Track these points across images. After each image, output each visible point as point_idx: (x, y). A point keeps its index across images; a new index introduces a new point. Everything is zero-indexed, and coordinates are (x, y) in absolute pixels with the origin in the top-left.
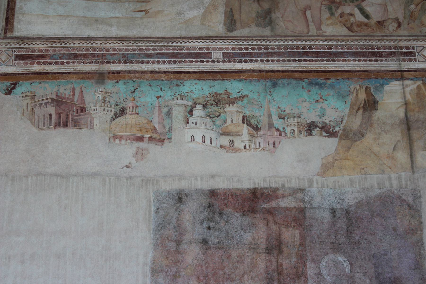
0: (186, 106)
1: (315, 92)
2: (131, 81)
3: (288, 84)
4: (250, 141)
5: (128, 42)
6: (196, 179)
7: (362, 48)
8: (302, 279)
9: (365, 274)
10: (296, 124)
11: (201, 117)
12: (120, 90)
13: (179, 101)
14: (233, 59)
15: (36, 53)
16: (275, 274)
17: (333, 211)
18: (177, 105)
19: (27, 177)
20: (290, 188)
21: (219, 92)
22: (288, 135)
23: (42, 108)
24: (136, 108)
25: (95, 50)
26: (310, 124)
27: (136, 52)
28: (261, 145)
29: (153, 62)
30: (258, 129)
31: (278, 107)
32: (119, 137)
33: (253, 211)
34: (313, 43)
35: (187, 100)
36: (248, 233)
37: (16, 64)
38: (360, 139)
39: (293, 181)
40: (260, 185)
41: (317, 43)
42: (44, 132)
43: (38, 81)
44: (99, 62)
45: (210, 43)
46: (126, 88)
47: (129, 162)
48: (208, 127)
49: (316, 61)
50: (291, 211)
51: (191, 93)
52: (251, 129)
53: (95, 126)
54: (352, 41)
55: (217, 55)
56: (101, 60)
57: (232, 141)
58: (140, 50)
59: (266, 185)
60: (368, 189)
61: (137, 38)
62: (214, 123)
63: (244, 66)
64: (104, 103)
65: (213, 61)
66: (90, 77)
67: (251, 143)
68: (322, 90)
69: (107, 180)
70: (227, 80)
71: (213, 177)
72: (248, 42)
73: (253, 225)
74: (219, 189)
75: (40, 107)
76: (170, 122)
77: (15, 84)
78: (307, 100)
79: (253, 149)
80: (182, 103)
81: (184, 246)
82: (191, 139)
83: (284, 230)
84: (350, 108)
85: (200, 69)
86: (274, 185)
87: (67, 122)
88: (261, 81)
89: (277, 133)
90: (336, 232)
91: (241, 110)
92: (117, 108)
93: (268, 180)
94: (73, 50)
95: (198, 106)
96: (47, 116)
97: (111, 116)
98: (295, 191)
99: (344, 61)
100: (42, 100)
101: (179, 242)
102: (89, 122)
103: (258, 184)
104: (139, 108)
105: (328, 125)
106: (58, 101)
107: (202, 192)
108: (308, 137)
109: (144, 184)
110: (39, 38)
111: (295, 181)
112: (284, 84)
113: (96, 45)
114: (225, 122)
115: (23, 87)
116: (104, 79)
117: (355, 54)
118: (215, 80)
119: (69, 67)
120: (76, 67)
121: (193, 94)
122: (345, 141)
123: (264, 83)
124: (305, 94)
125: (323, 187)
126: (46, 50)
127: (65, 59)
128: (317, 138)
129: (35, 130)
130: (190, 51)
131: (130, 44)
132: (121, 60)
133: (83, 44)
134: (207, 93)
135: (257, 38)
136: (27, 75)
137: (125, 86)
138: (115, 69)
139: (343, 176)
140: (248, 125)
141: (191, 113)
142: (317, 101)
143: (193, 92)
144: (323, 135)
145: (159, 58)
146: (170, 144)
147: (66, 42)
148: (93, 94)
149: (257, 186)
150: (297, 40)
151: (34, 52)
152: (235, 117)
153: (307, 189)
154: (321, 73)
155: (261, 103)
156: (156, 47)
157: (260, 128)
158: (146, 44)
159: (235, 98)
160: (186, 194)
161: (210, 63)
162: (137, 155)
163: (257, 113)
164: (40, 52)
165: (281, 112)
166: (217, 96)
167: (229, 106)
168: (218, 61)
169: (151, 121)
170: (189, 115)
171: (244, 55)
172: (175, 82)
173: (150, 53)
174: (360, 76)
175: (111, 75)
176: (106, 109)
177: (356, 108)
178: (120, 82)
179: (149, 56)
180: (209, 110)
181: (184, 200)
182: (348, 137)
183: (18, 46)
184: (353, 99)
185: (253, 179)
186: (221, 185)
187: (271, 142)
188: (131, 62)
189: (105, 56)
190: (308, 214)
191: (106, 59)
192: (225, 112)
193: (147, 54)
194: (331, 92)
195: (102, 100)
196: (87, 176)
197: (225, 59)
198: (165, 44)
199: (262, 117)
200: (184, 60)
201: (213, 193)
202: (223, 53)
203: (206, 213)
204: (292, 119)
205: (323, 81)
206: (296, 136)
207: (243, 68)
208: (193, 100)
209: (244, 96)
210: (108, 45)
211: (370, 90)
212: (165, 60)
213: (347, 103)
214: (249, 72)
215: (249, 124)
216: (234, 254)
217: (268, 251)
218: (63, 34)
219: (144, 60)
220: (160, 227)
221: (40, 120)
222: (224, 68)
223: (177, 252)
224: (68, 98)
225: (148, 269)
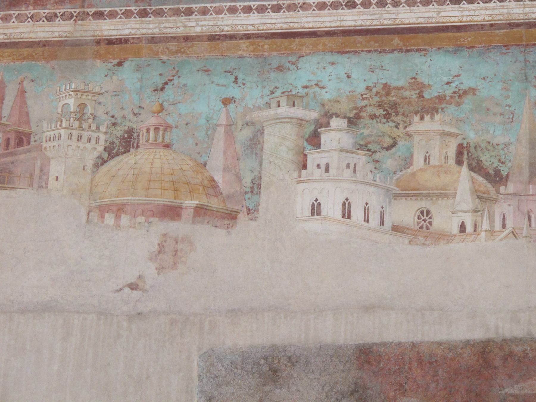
0: (301, 122)
4: (476, 211)
11: (342, 150)
13: (285, 110)
18: (278, 120)
21: (394, 84)
24: (165, 130)
28: (507, 222)
29: (219, 11)
30: (501, 179)
32: (115, 208)
35: (307, 107)
40: (500, 331)
44: (72, 16)
46: (141, 80)
47: (137, 274)
48: (359, 176)
51: (317, 89)
52: (480, 179)
53: (52, 182)
56: (78, 10)
57: (425, 213)
59: (519, 332)
62: (378, 165)
63: (466, 13)
66: (46, 54)
67: (479, 219)
70: (419, 50)
71: (368, 309)
74: (384, 344)
80: (292, 115)
82: (313, 209)
85: (344, 24)
91: (454, 130)
92: (115, 132)
95: (335, 122)
97: (96, 154)
102: (37, 172)
103: (497, 328)
104: (174, 130)
107: (336, 352)
114: (408, 161)
118: (384, 51)
120: (11, 31)
121: (324, 91)
123: (521, 58)
132: (133, 8)
134: (361, 88)
137: (138, 75)
138: (114, 33)
140: (471, 168)
141: (314, 140)
143: (321, 84)
146: (253, 224)
149: (491, 335)
152: (437, 150)
155: (512, 109)
157: (507, 176)
159: (438, 97)
160: (290, 358)
162: (160, 256)
163: (498, 135)
166: (388, 94)
167: (422, 118)
169: (205, 165)
170: (309, 147)
175: (103, 46)
176: (86, 135)
178: (126, 64)
180: (366, 132)
181: (285, 374)
186: (392, 330)
188: (159, 13)
191: (91, 6)
192: (410, 136)
195: (75, 113)
196: (23, 312)
199: (512, 148)
201: (366, 355)
207: (465, 19)
208: (323, 105)
209: (465, 92)
212: (251, 4)
215: (477, 167)
219: (194, 6)
222: (412, 21)
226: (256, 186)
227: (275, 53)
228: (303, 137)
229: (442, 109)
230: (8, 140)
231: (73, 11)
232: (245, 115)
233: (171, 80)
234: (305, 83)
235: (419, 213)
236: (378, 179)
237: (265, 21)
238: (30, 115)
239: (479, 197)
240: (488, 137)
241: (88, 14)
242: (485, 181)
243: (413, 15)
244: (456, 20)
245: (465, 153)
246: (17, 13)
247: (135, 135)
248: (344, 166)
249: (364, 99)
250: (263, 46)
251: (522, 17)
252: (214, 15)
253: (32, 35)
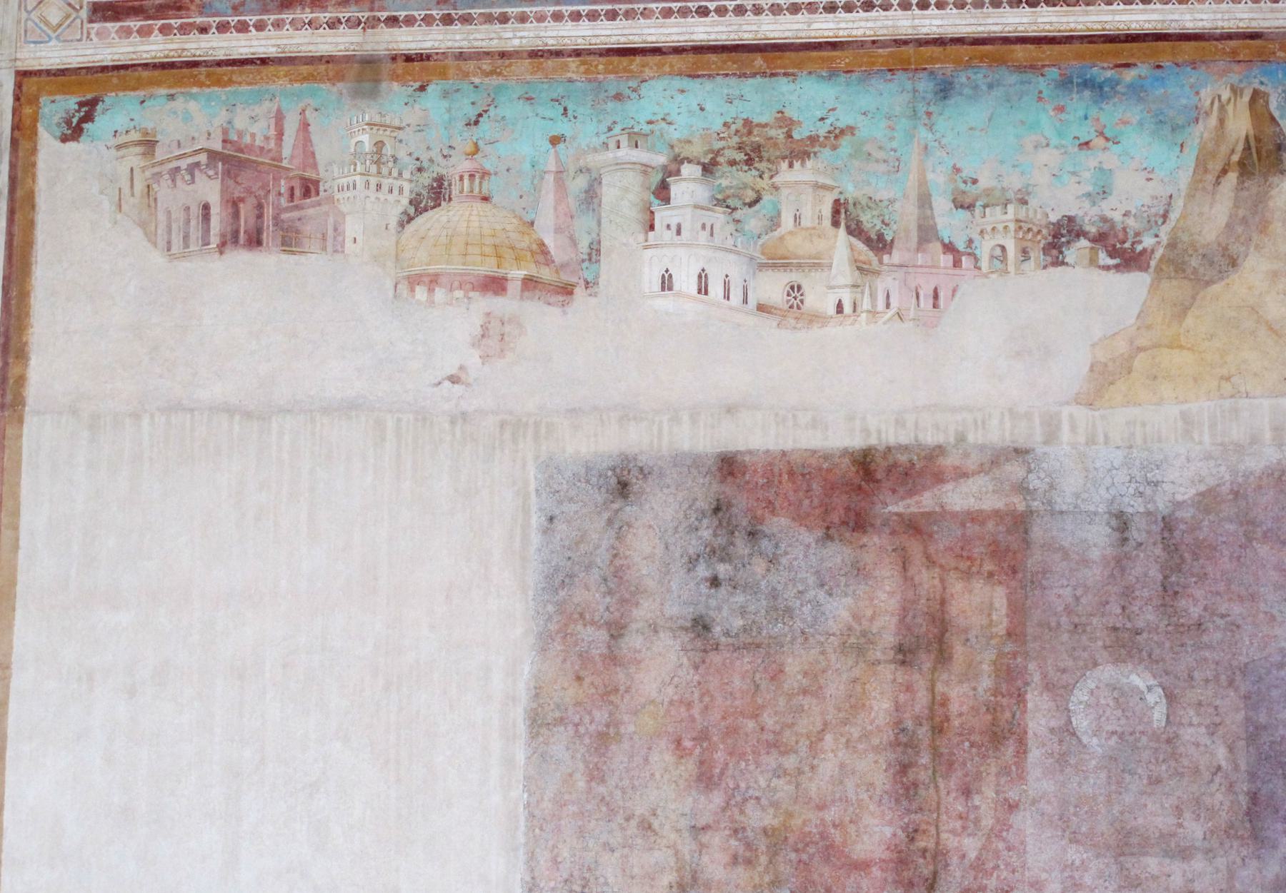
0: (646, 169)
1: (1081, 113)
2: (465, 86)
3: (990, 86)
6: (675, 419)
8: (1009, 750)
9: (1213, 729)
10: (1012, 226)
11: (696, 207)
13: (626, 153)
16: (923, 732)
17: (1122, 523)
18: (619, 165)
19: (136, 416)
20: (982, 448)
21: (756, 121)
22: (984, 264)
23: (179, 182)
24: (482, 178)
26: (1058, 225)
28: (892, 300)
29: (541, 18)
30: (885, 246)
31: (954, 167)
32: (426, 280)
33: (859, 523)
35: (652, 149)
36: (841, 596)
37: (93, 36)
38: (1222, 275)
39: (995, 422)
40: (883, 436)
42: (185, 265)
43: (163, 91)
46: (449, 110)
47: (457, 366)
48: (717, 240)
50: (983, 523)
51: (663, 124)
52: (860, 246)
53: (349, 244)
56: (367, 14)
57: (795, 289)
59: (904, 438)
60: (1239, 448)
62: (739, 226)
63: (843, 25)
64: (378, 162)
67: (859, 296)
68: (1103, 106)
69: (390, 424)
70: (785, 74)
71: (730, 410)
73: (859, 571)
74: (750, 452)
75: (173, 180)
76: (594, 224)
77: (93, 103)
78: (1054, 141)
79: (864, 315)
80: (634, 160)
81: (633, 641)
82: (663, 282)
83: (957, 587)
84: (1197, 166)
85: (694, 37)
86: (930, 438)
87: (259, 231)
88: (900, 75)
89: (946, 260)
90: (1128, 593)
91: (829, 182)
92: (421, 180)
93: (910, 419)
95: (687, 169)
96: (196, 211)
97: (401, 209)
98: (998, 457)
100: (179, 157)
101: (616, 630)
102: (330, 232)
103: (879, 432)
104: (493, 177)
105: (1119, 227)
106: (231, 160)
107: (694, 462)
108: (1051, 269)
109: (507, 435)
111: (1002, 422)
112: (976, 87)
114: (774, 222)
115: (119, 114)
116: (377, 81)
118: (744, 75)
119: (263, 42)
120: (285, 41)
122: (1174, 283)
124: (1046, 119)
125: (1091, 441)
127: (252, 12)
128: (1079, 272)
129: (157, 258)
132: (434, 13)
134: (717, 125)
136: (129, 72)
137: (445, 104)
138: (413, 46)
139: (1160, 402)
140: (850, 232)
141: (663, 192)
142: (1087, 143)
143: (669, 119)
144: (1101, 263)
146: (593, 300)
148: (341, 134)
149: (873, 441)
152: (809, 207)
153: (1040, 450)
154: (1102, 46)
155: (898, 154)
157: (892, 241)
159: (810, 138)
160: (641, 469)
162: (484, 341)
163: (883, 191)
165: (962, 186)
166: (750, 133)
167: (791, 166)
169: (532, 223)
170: (657, 202)
172: (613, 84)
174: (1234, 52)
175: (401, 64)
176: (386, 182)
177: (1216, 166)
178: (430, 89)
181: (636, 488)
182: (1184, 271)
184: (1206, 135)
185: (864, 419)
186: (756, 436)
187: (926, 291)
188: (466, 20)
190: (1037, 533)
191: (382, 9)
192: (776, 188)
194: (1135, 113)
195: (373, 153)
196: (326, 411)
199: (897, 205)
200: (642, 6)
201: (729, 466)
203: (706, 534)
204: (998, 208)
205: (1109, 74)
206: (1011, 268)
207: (841, 33)
208: (672, 147)
209: (842, 132)
211: (1267, 103)
212: (580, 8)
213: (1186, 150)
214: (862, 44)
215: (856, 230)
216: (793, 667)
217: (904, 655)
219: (509, 10)
220: (559, 580)
221: (174, 226)
223: (613, 659)
224: (262, 148)
225: (519, 715)
226: (594, 253)
227: (612, 76)
228: (649, 189)
229: (815, 153)
230: (292, 189)
231: (360, 15)
232: (578, 159)
233: (486, 111)
234: (650, 118)
235: (788, 288)
236: (739, 245)
237: (598, 32)
238: (318, 156)
239: (858, 268)
240: (868, 191)
242: (866, 248)
243: (778, 27)
244: (831, 34)
245: (843, 211)
246: (291, 17)
247: (446, 183)
248: (699, 226)
249: (722, 139)
250: (596, 66)
251: (910, 31)
252: (535, 24)
253: (311, 48)
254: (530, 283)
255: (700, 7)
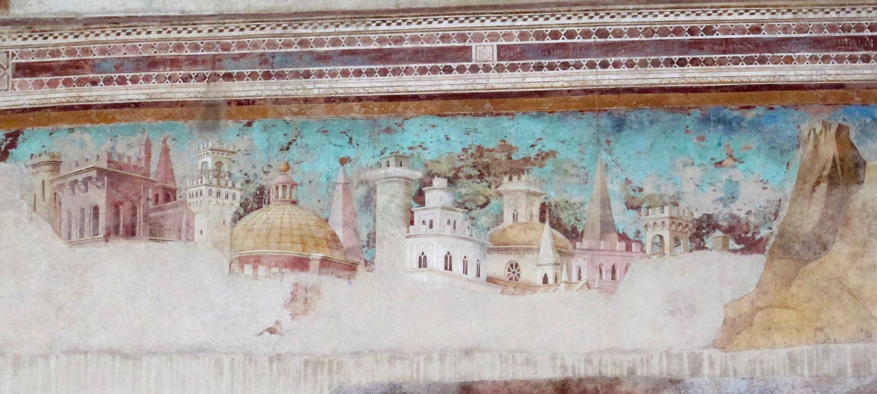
0: (407, 181)
1: (716, 142)
2: (280, 123)
3: (652, 122)
4: (556, 264)
5: (274, 25)
6: (429, 359)
7: (832, 28)
10: (667, 222)
11: (443, 208)
12: (251, 147)
13: (394, 170)
14: (521, 62)
15: (61, 59)
18: (388, 179)
19: (46, 357)
20: (647, 379)
21: (487, 146)
22: (648, 248)
23: (77, 191)
25: (196, 47)
26: (700, 221)
27: (293, 50)
29: (333, 75)
31: (626, 179)
32: (252, 260)
34: (714, 17)
35: (412, 167)
37: (16, 87)
38: (817, 256)
39: (655, 361)
40: (577, 371)
41: (725, 17)
42: (81, 250)
43: (66, 126)
44: (205, 78)
45: (467, 24)
46: (268, 140)
47: (274, 321)
48: (459, 232)
49: (722, 62)
51: (420, 150)
52: (559, 235)
53: (197, 234)
54: (810, 10)
55: (484, 52)
56: (210, 72)
57: (514, 266)
58: (302, 43)
59: (591, 372)
60: (829, 379)
61: (296, 14)
62: (474, 222)
63: (547, 79)
64: (217, 177)
65: (474, 69)
66: (184, 114)
67: (559, 271)
68: (732, 136)
69: (226, 362)
70: (507, 114)
71: (468, 352)
72: (558, 19)
74: (482, 382)
75: (73, 190)
76: (371, 221)
78: (697, 162)
79: (562, 285)
80: (400, 175)
82: (420, 262)
84: (799, 178)
85: (442, 88)
87: (133, 226)
88: (588, 114)
89: (620, 246)
91: (538, 190)
92: (249, 189)
93: (596, 359)
94: (146, 48)
95: (437, 182)
96: (89, 211)
97: (234, 210)
98: (658, 385)
99: (789, 60)
100: (77, 173)
102: (184, 226)
103: (574, 368)
104: (299, 187)
105: (743, 222)
106: (113, 175)
108: (695, 252)
109: (310, 371)
110: (68, 21)
111: (661, 361)
112: (641, 123)
113: (198, 35)
114: (499, 218)
115: (34, 143)
116: (218, 119)
117: (817, 43)
118: (476, 115)
119: (137, 92)
120: (152, 91)
121: (427, 152)
122: (783, 261)
123: (594, 122)
124: (691, 146)
125: (724, 374)
126: (83, 49)
128: (715, 254)
129: (60, 245)
130: (420, 45)
131: (279, 30)
132: (257, 70)
133: (169, 32)
134: (458, 150)
135: (579, 8)
136: (42, 112)
137: (265, 135)
138: (243, 94)
139: (773, 346)
140: (553, 226)
141: (420, 198)
142: (720, 163)
143: (424, 146)
144: (731, 247)
145: (346, 64)
146: (370, 275)
147: (129, 30)
148: (192, 157)
149: (569, 374)
150: (677, 11)
151: (58, 56)
152: (524, 207)
153: (688, 380)
154: (731, 94)
155: (587, 170)
156: (340, 37)
157: (582, 232)
158: (315, 28)
161: (468, 74)
162: (293, 304)
163: (576, 197)
164: (71, 55)
165: (632, 193)
166: (481, 156)
167: (511, 179)
168: (487, 69)
169: (327, 220)
170: (415, 205)
171: (547, 51)
172: (384, 121)
173: (326, 52)
174: (824, 98)
176: (224, 191)
177: (812, 179)
178: (255, 125)
179: (324, 58)
180: (463, 191)
182: (790, 253)
183: (19, 42)
184: (805, 157)
185: (563, 358)
187: (607, 268)
188: (281, 75)
189: (219, 60)
192: (500, 195)
193: (318, 53)
194: (754, 141)
195: (214, 170)
196: (180, 353)
197: (504, 63)
198: (361, 29)
199: (586, 207)
200: (405, 66)
202: (499, 47)
204: (658, 209)
205: (736, 113)
206: (667, 251)
207: (546, 85)
208: (426, 166)
209: (547, 155)
210: (226, 33)
211: (848, 134)
212: (361, 67)
213: (791, 168)
214: (560, 93)
215: (557, 225)
218: (123, 8)
219: (311, 69)
221: (73, 221)
222: (500, 86)
224: (135, 167)
226: (371, 241)
227: (384, 116)
228: (410, 195)
229: (528, 170)
230: (157, 195)
231: (205, 72)
232: (360, 174)
233: (294, 140)
234: (410, 145)
235: (508, 266)
236: (474, 235)
237: (374, 85)
238: (175, 173)
239: (559, 252)
240: (566, 196)
241: (219, 75)
242: (563, 237)
243: (501, 80)
244: (539, 86)
245: (547, 211)
246: (156, 73)
247: (266, 192)
248: (446, 222)
249: (462, 160)
250: (373, 108)
251: (595, 84)
252: (329, 78)
253: (170, 95)
254: (325, 262)
255: (446, 67)
